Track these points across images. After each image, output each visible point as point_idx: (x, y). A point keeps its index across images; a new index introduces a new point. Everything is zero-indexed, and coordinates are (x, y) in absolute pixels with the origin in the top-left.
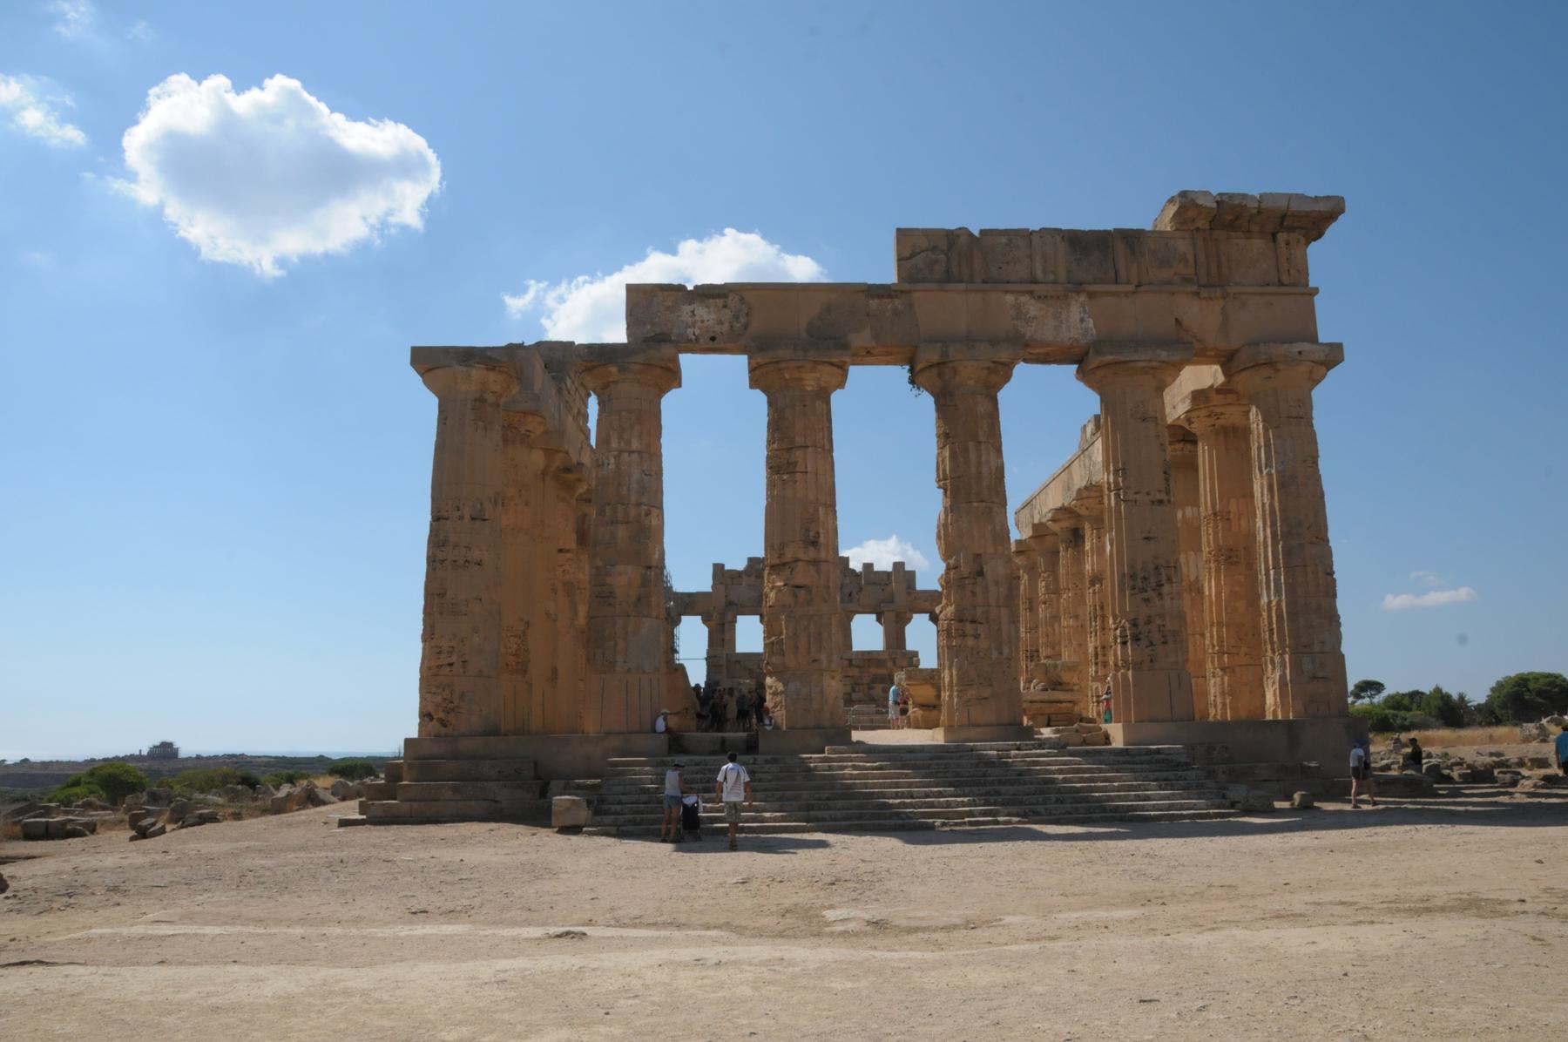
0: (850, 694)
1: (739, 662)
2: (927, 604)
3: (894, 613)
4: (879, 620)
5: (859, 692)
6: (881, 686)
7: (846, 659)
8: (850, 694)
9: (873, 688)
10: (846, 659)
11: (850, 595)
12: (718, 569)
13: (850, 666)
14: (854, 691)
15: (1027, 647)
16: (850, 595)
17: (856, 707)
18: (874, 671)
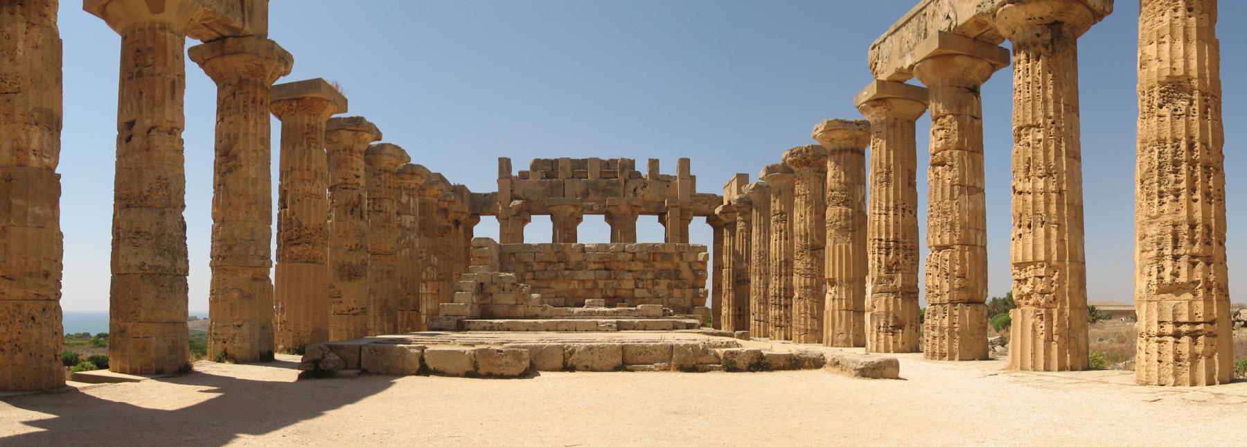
0: (633, 290)
1: (514, 254)
2: (706, 206)
3: (679, 209)
4: (660, 220)
5: (643, 288)
6: (667, 281)
7: (629, 253)
8: (633, 290)
9: (657, 284)
10: (629, 253)
11: (635, 191)
12: (505, 164)
13: (633, 260)
14: (637, 287)
15: (880, 234)
16: (635, 191)
17: (639, 307)
18: (659, 265)
